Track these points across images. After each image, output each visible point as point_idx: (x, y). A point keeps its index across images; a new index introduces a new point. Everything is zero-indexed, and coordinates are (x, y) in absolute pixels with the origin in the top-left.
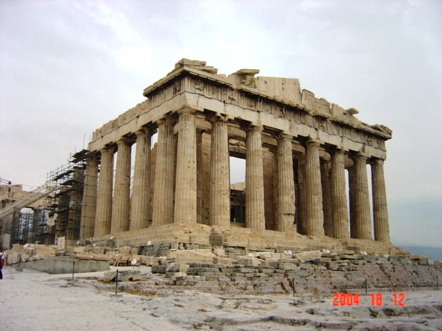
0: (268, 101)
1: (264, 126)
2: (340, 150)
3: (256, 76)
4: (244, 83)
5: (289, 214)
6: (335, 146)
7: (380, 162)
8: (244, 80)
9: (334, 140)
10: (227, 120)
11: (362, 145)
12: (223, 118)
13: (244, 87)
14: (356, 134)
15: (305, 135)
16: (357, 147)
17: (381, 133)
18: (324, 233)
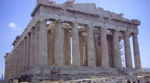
0: (78, 13)
1: (79, 23)
2: (116, 31)
3: (74, 3)
4: (68, 6)
5: (92, 59)
6: (114, 29)
7: (135, 35)
8: (68, 5)
9: (113, 27)
10: (61, 22)
11: (127, 28)
12: (58, 21)
13: (67, 8)
14: (124, 24)
15: (99, 26)
16: (124, 29)
17: (135, 22)
18: (109, 66)
